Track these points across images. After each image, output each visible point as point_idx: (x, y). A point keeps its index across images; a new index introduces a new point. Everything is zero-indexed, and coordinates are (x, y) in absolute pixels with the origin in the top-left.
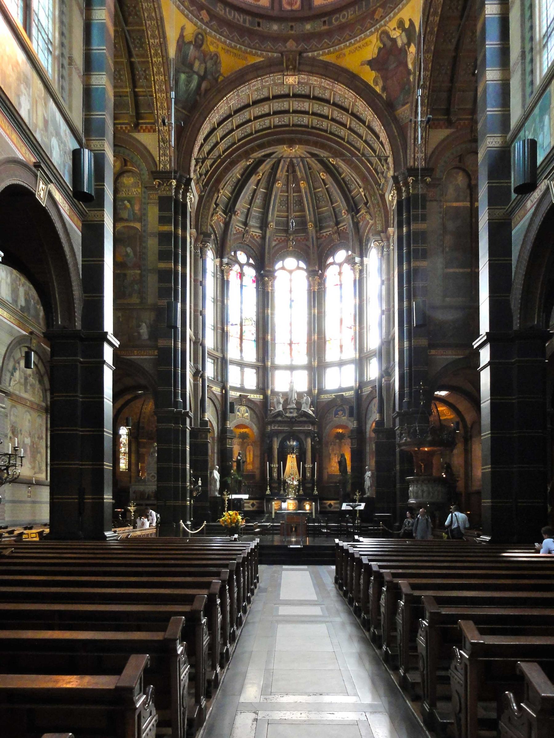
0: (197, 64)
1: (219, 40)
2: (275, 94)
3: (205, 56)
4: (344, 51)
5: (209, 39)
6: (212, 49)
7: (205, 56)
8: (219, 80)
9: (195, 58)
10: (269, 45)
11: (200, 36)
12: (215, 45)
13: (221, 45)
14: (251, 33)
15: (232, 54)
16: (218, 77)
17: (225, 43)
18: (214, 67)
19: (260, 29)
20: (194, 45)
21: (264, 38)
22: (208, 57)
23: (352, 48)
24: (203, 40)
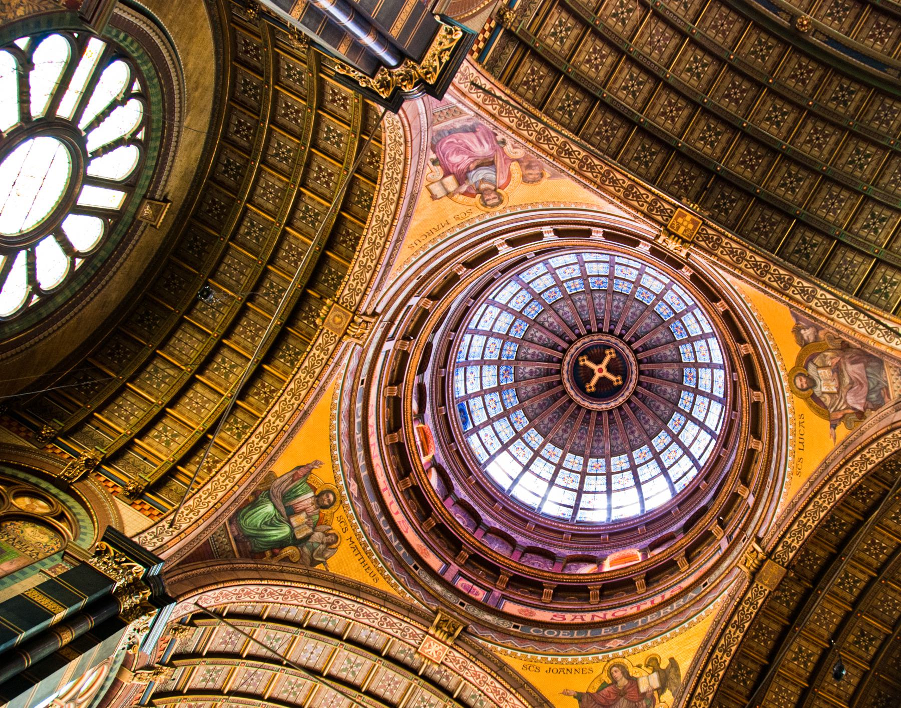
0: (303, 515)
1: (354, 528)
2: (372, 688)
3: (319, 523)
4: (538, 664)
5: (340, 512)
6: (336, 527)
7: (319, 523)
8: (317, 567)
9: (304, 510)
10: (419, 594)
11: (331, 497)
12: (342, 524)
13: (350, 532)
14: (400, 564)
15: (359, 557)
16: (320, 562)
17: (359, 537)
18: (322, 547)
19: (417, 572)
20: (315, 496)
21: (416, 584)
22: (323, 528)
23: (552, 666)
24: (331, 504)
